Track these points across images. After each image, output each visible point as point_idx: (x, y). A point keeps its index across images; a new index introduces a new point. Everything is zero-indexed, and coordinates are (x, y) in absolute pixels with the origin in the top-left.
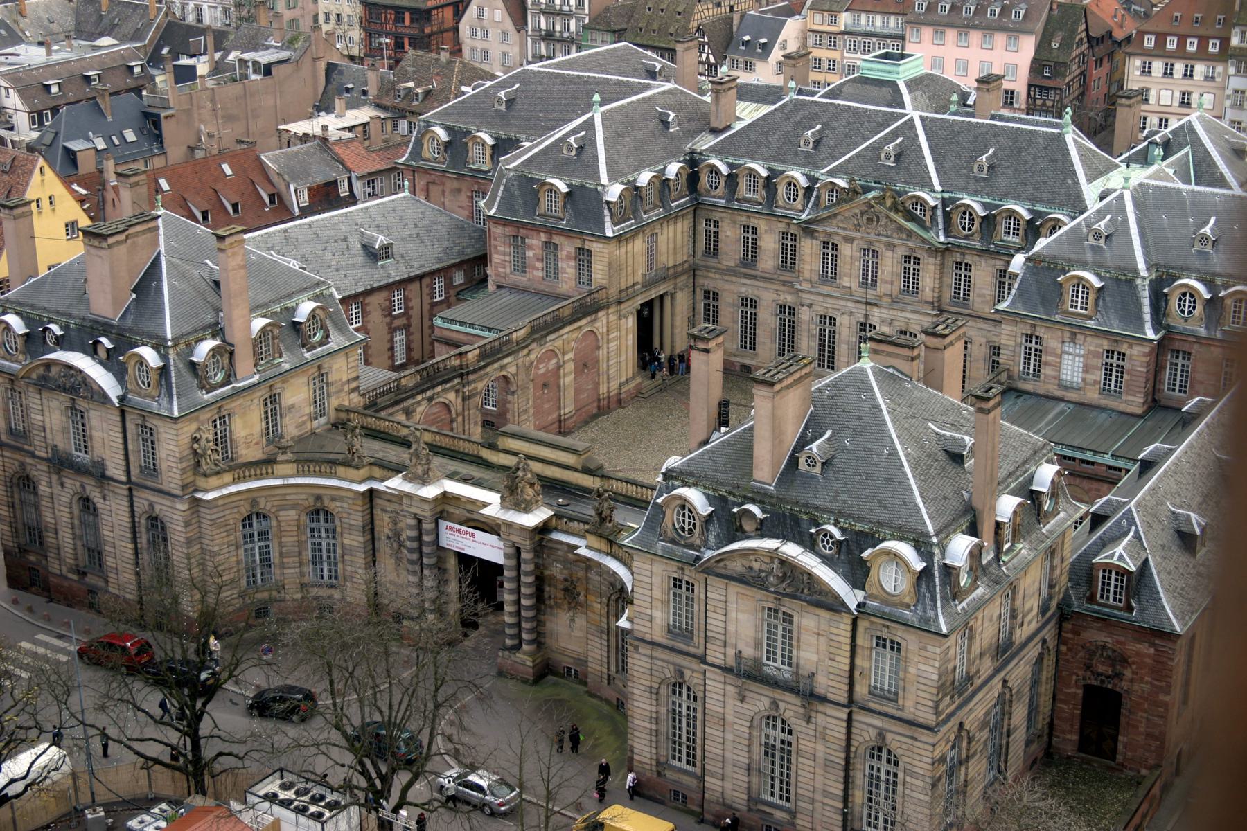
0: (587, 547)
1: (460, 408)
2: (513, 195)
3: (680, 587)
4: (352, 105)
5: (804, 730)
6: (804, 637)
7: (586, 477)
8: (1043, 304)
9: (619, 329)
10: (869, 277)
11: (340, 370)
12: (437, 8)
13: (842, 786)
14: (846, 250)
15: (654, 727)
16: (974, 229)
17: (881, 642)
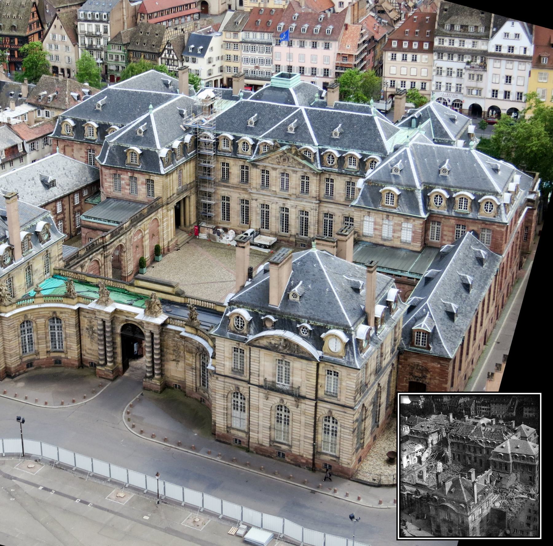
0: (185, 332)
1: (103, 262)
2: (113, 155)
3: (237, 351)
4: (18, 104)
5: (295, 411)
6: (295, 371)
7: (177, 297)
8: (373, 202)
9: (167, 216)
10: (285, 186)
11: (55, 252)
12: (31, 35)
13: (313, 434)
14: (274, 175)
15: (225, 412)
16: (334, 163)
17: (329, 372)
